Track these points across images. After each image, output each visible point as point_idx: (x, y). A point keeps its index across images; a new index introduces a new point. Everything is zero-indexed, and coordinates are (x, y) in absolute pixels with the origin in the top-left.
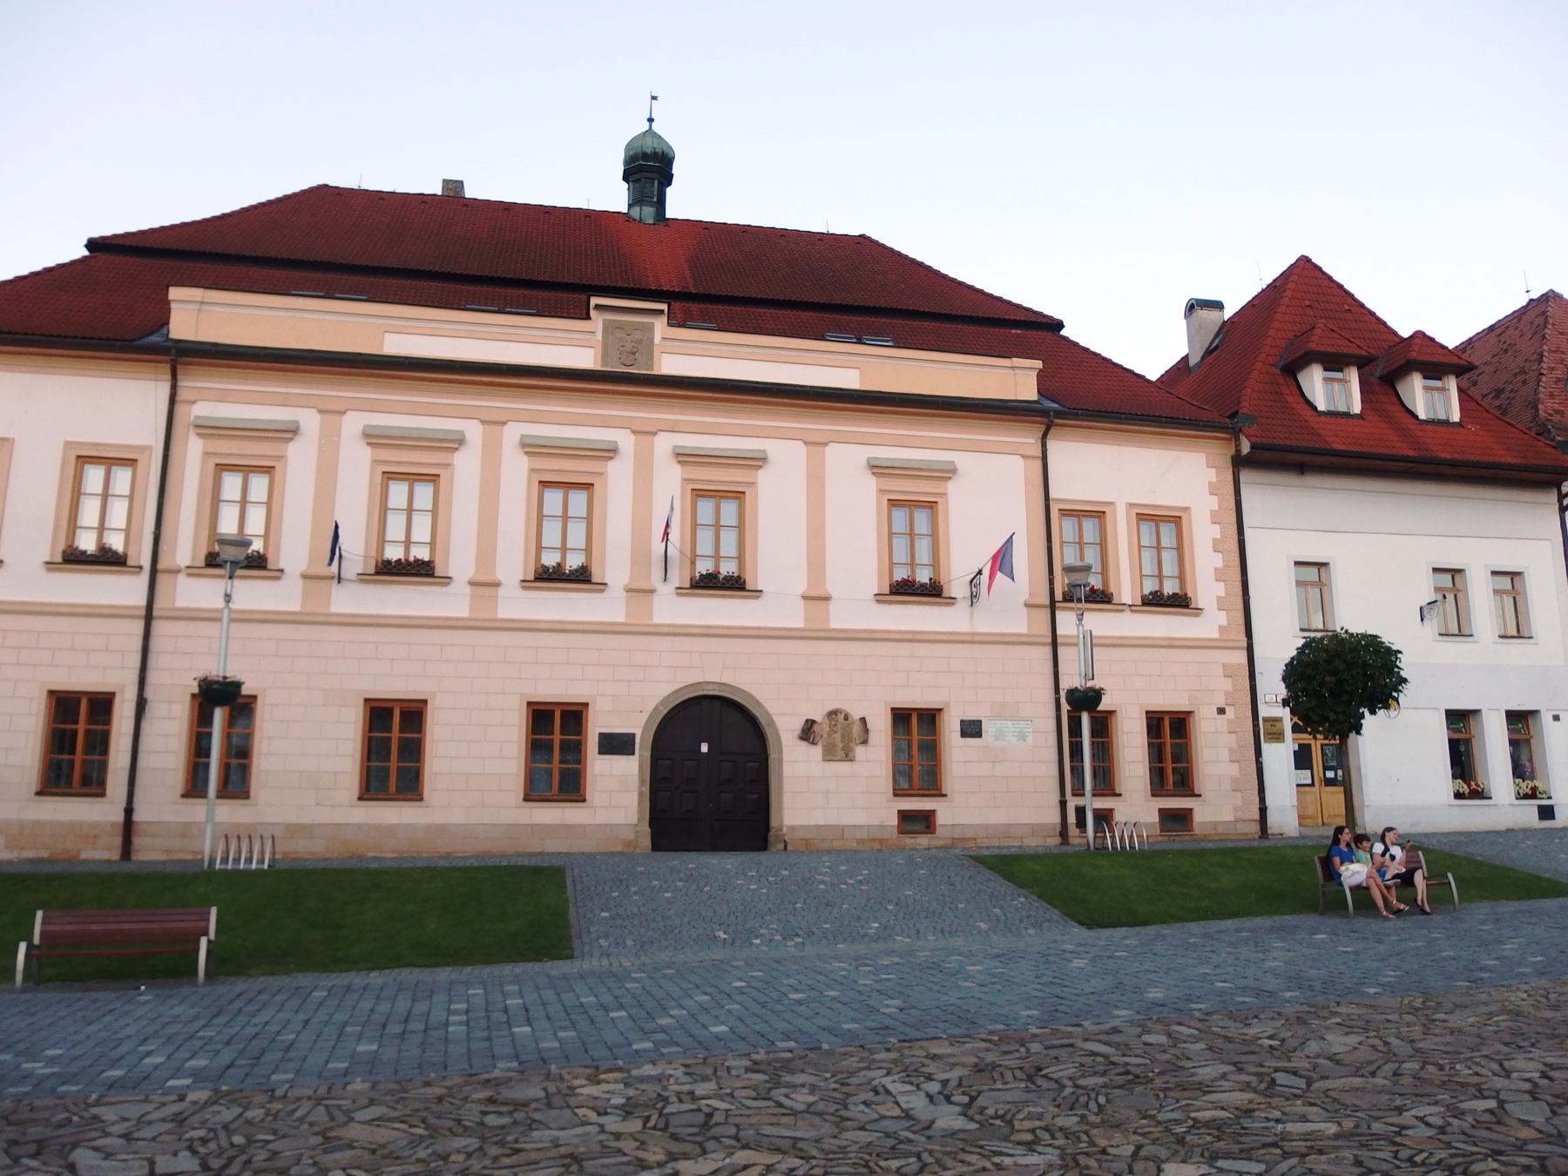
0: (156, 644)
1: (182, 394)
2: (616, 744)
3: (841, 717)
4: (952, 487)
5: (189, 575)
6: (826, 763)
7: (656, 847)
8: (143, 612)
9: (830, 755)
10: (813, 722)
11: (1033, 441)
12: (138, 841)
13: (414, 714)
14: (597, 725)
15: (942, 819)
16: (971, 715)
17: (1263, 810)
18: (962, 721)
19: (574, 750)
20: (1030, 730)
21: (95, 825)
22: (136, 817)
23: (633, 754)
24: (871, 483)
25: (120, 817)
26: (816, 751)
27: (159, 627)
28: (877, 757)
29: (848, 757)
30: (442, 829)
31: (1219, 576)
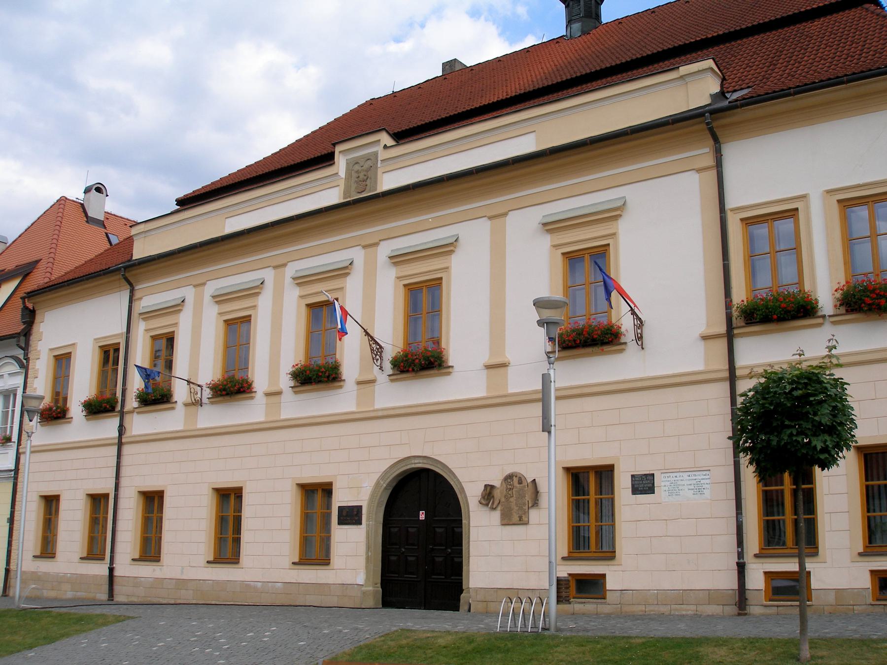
0: (125, 460)
1: (137, 295)
2: (350, 516)
3: (515, 480)
4: (623, 227)
5: (138, 413)
6: (503, 527)
7: (387, 602)
8: (117, 441)
9: (507, 520)
10: (492, 487)
11: (707, 150)
12: (117, 588)
14: (341, 498)
15: (611, 584)
16: (642, 469)
18: (633, 476)
20: (708, 481)
22: (117, 573)
23: (360, 523)
24: (546, 241)
25: (107, 572)
26: (496, 515)
27: (126, 449)
29: (523, 521)
30: (246, 586)
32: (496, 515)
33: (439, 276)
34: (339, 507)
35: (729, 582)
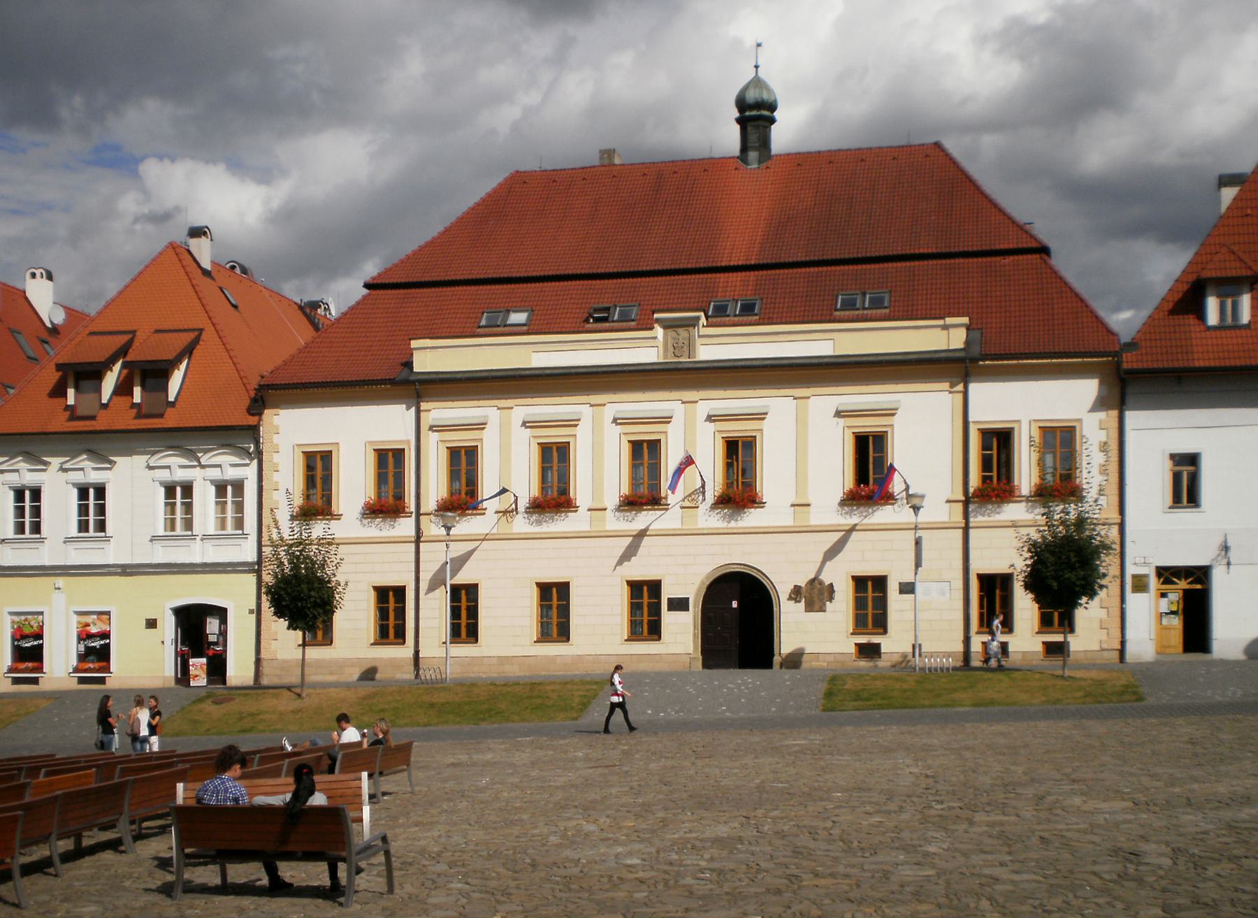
2: (679, 604)
4: (896, 421)
7: (707, 664)
9: (810, 607)
10: (800, 587)
13: (563, 588)
14: (667, 593)
17: (1123, 643)
18: (900, 583)
19: (655, 610)
21: (402, 659)
28: (842, 606)
29: (822, 609)
30: (580, 657)
31: (1104, 470)
32: (802, 604)
33: (754, 435)
34: (668, 599)
35: (959, 647)
